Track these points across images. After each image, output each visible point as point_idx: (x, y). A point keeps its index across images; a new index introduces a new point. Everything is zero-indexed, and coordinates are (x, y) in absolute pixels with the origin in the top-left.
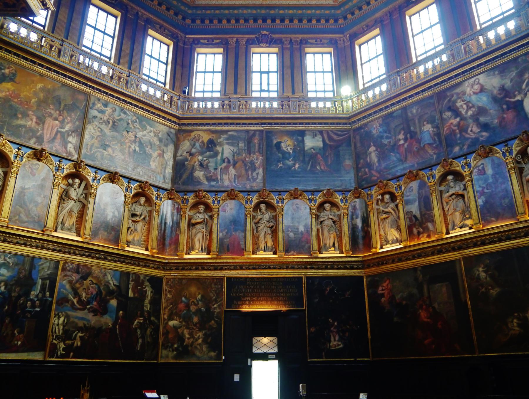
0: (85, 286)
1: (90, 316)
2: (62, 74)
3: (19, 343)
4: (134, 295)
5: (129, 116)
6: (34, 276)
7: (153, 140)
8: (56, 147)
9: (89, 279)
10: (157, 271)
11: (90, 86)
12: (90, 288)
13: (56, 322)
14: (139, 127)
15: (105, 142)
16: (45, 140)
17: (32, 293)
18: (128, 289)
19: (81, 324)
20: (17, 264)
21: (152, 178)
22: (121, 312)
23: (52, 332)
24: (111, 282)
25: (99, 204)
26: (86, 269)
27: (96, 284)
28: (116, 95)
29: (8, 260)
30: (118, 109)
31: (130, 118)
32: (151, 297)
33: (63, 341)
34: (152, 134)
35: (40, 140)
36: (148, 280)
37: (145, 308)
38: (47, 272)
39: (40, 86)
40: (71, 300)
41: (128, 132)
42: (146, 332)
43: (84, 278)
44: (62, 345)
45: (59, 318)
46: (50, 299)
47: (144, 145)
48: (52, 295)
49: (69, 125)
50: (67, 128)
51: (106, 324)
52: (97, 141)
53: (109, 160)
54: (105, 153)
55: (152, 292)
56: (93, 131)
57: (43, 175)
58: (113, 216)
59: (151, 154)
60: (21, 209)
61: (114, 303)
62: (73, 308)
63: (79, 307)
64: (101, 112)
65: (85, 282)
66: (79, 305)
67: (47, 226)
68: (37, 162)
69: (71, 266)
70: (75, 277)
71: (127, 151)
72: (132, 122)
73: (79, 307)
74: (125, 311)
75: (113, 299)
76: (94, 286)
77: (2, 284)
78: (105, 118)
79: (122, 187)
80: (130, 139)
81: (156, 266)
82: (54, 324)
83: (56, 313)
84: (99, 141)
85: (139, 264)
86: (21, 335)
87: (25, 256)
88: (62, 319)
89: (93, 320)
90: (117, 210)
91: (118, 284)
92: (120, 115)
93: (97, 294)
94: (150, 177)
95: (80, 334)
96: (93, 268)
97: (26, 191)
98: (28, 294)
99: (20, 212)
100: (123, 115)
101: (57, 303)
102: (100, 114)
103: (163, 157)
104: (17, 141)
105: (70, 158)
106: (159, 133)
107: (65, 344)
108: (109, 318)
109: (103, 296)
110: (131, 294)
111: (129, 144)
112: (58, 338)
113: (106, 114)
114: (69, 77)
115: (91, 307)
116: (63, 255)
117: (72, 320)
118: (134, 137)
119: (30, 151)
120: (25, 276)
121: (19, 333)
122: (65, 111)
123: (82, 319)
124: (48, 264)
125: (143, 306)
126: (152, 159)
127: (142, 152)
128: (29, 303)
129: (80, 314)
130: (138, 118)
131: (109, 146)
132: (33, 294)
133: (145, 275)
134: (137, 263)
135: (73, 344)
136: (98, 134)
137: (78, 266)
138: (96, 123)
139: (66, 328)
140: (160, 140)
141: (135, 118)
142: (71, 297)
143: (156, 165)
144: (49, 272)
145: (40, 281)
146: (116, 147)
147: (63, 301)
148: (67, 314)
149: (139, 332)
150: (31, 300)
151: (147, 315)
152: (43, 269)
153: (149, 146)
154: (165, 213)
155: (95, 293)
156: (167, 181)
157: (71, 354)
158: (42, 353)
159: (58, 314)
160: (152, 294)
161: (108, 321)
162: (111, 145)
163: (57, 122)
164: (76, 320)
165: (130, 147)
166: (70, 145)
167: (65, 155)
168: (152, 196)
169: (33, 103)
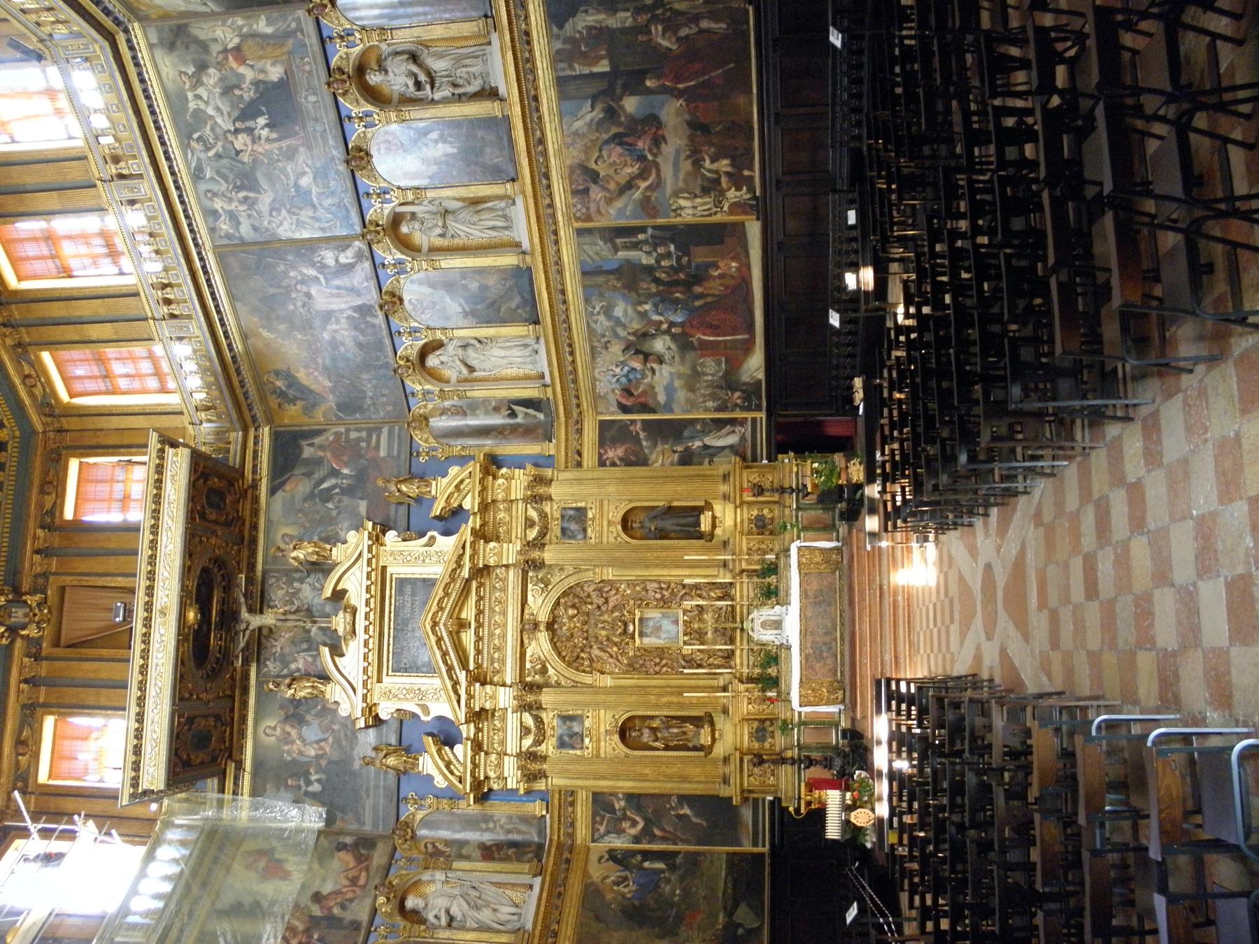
0: (611, 172)
1: (668, 150)
2: (219, 312)
3: (734, 264)
4: (602, 58)
5: (199, 159)
6: (615, 266)
7: (214, 87)
8: (362, 275)
9: (593, 166)
10: (531, 7)
11: (201, 259)
12: (612, 160)
13: (690, 211)
14: (208, 127)
15: (293, 197)
16: (360, 303)
17: (644, 262)
18: (593, 76)
19: (687, 166)
20: (601, 295)
21: (307, 68)
22: (648, 83)
23: (710, 215)
24: (588, 117)
25: (430, 177)
26: (575, 177)
27: (600, 150)
28: (179, 208)
29: (597, 309)
30: (203, 187)
31: (202, 156)
32: (599, 12)
33: (722, 193)
34: (201, 91)
35: (363, 310)
36: (561, 27)
37: (627, 25)
38: (599, 250)
39: (265, 334)
40: (643, 194)
41: (238, 153)
42: (681, 13)
43: (594, 177)
44: (732, 194)
45: (681, 208)
46: (650, 231)
47: (241, 106)
48: (643, 229)
49: (305, 271)
50: (311, 272)
51: (678, 113)
52: (303, 213)
53: (326, 177)
54: (314, 190)
55: (586, 12)
56: (286, 225)
57: (426, 290)
58: (445, 142)
59: (252, 84)
60: (503, 310)
61: (631, 104)
62: (658, 185)
63: (653, 176)
64: (233, 217)
65: (602, 174)
66: (650, 175)
67: (516, 263)
68: (406, 303)
69: (579, 206)
70: (596, 193)
71: (284, 144)
72: (208, 149)
73: (653, 176)
74: (642, 74)
75: (622, 107)
76: (605, 153)
77: (640, 309)
78: (242, 208)
79: (369, 135)
80: (249, 142)
81: (519, 12)
82: (694, 215)
83: (673, 214)
84: (301, 209)
85: (528, 61)
86: (721, 264)
87: (584, 287)
88: (682, 203)
89: (676, 140)
90: (426, 134)
91: (589, 102)
92: (212, 179)
93: (621, 144)
94: (310, 72)
95: (707, 164)
96: (568, 162)
97: (467, 309)
98: (649, 270)
99: (509, 308)
100: (209, 173)
101: (654, 217)
102: (241, 219)
103: (238, 49)
104: (387, 341)
105: (367, 254)
106: (186, 74)
107: (729, 189)
108: (666, 109)
109: (621, 130)
110: (603, 67)
111: (262, 142)
112: (718, 204)
113: (233, 207)
114: (214, 299)
115: (650, 151)
116: (561, 224)
117: (681, 184)
118: (240, 137)
119: (395, 321)
120: (618, 279)
121: (718, 267)
122: (284, 284)
123: (676, 164)
124: (585, 247)
125: (623, 31)
126: (261, 77)
127: (263, 109)
128: (663, 264)
129: (667, 171)
130: (190, 137)
131: (297, 186)
132: (647, 260)
133: (551, 37)
134: (528, 65)
135: (728, 174)
136: (284, 213)
137: (575, 193)
138: (266, 223)
139: (698, 192)
140: (202, 67)
141: (193, 144)
142: (637, 195)
143: (273, 65)
144: (601, 243)
145: (620, 253)
146: (289, 169)
147: (647, 206)
148: (671, 196)
149: (684, 32)
150: (658, 261)
151: (644, 17)
152: (597, 254)
153: (237, 92)
154: (377, 12)
155: (619, 149)
156: (293, 25)
157: (746, 173)
158: (747, 224)
159: (675, 211)
160: (591, 11)
161: (673, 110)
162: (292, 183)
163: (313, 292)
164: (681, 176)
165: (268, 140)
166: (343, 259)
167: (367, 265)
168: (352, 58)
169: (305, 335)
